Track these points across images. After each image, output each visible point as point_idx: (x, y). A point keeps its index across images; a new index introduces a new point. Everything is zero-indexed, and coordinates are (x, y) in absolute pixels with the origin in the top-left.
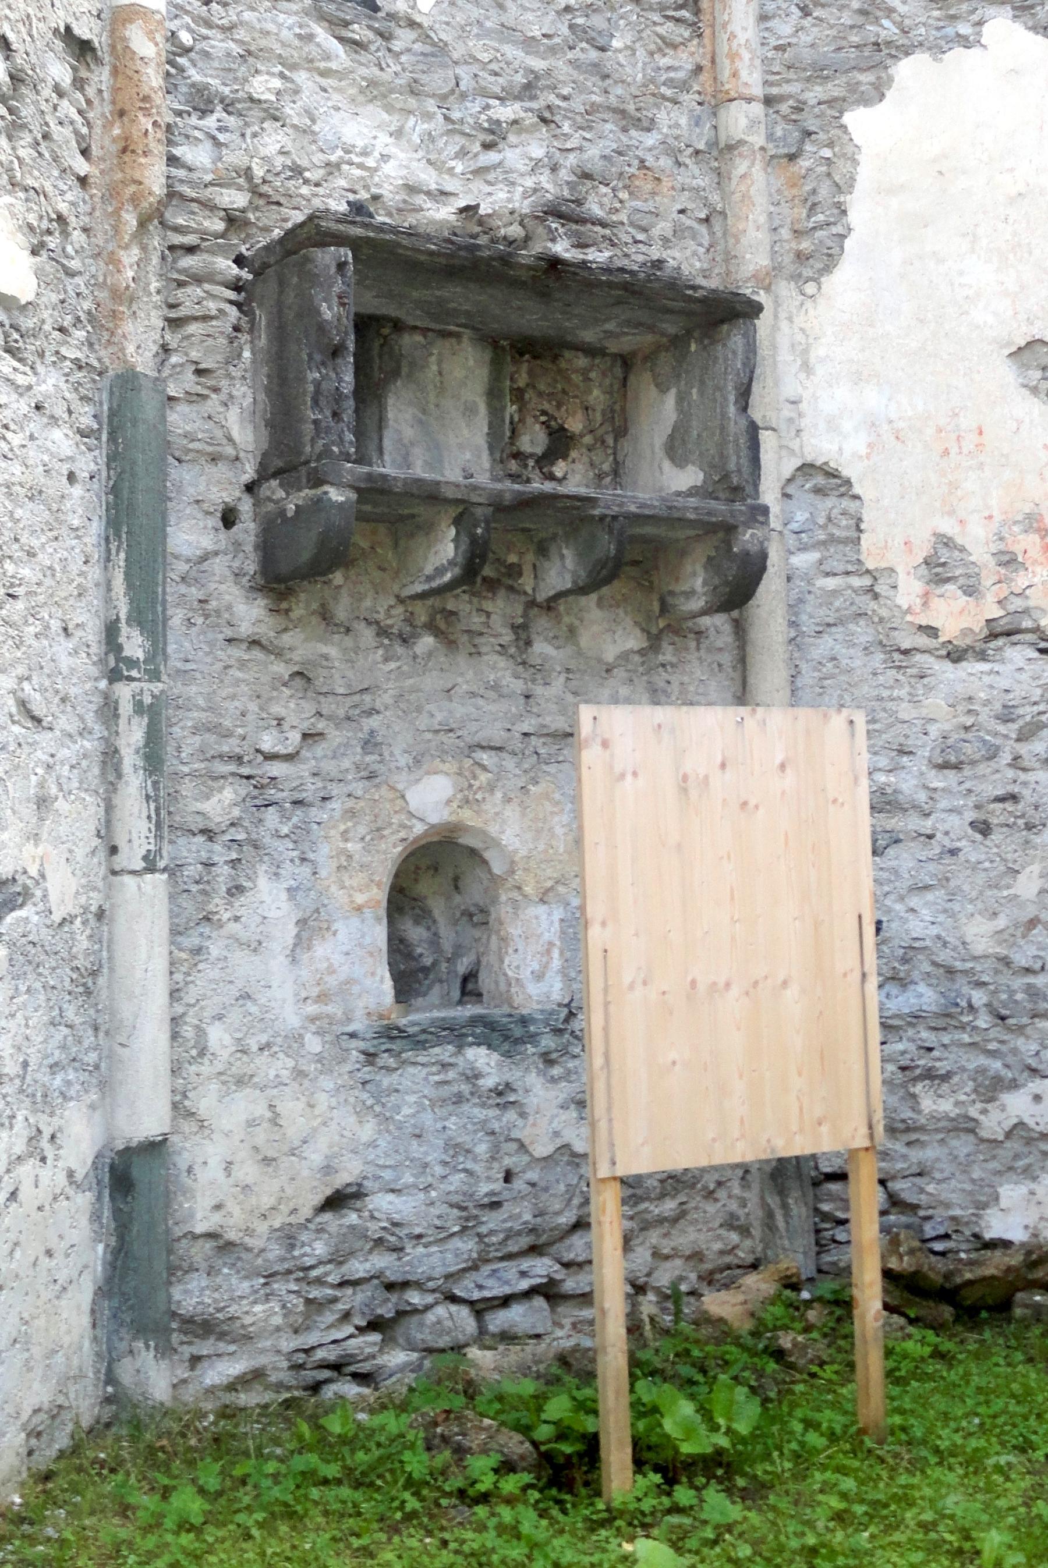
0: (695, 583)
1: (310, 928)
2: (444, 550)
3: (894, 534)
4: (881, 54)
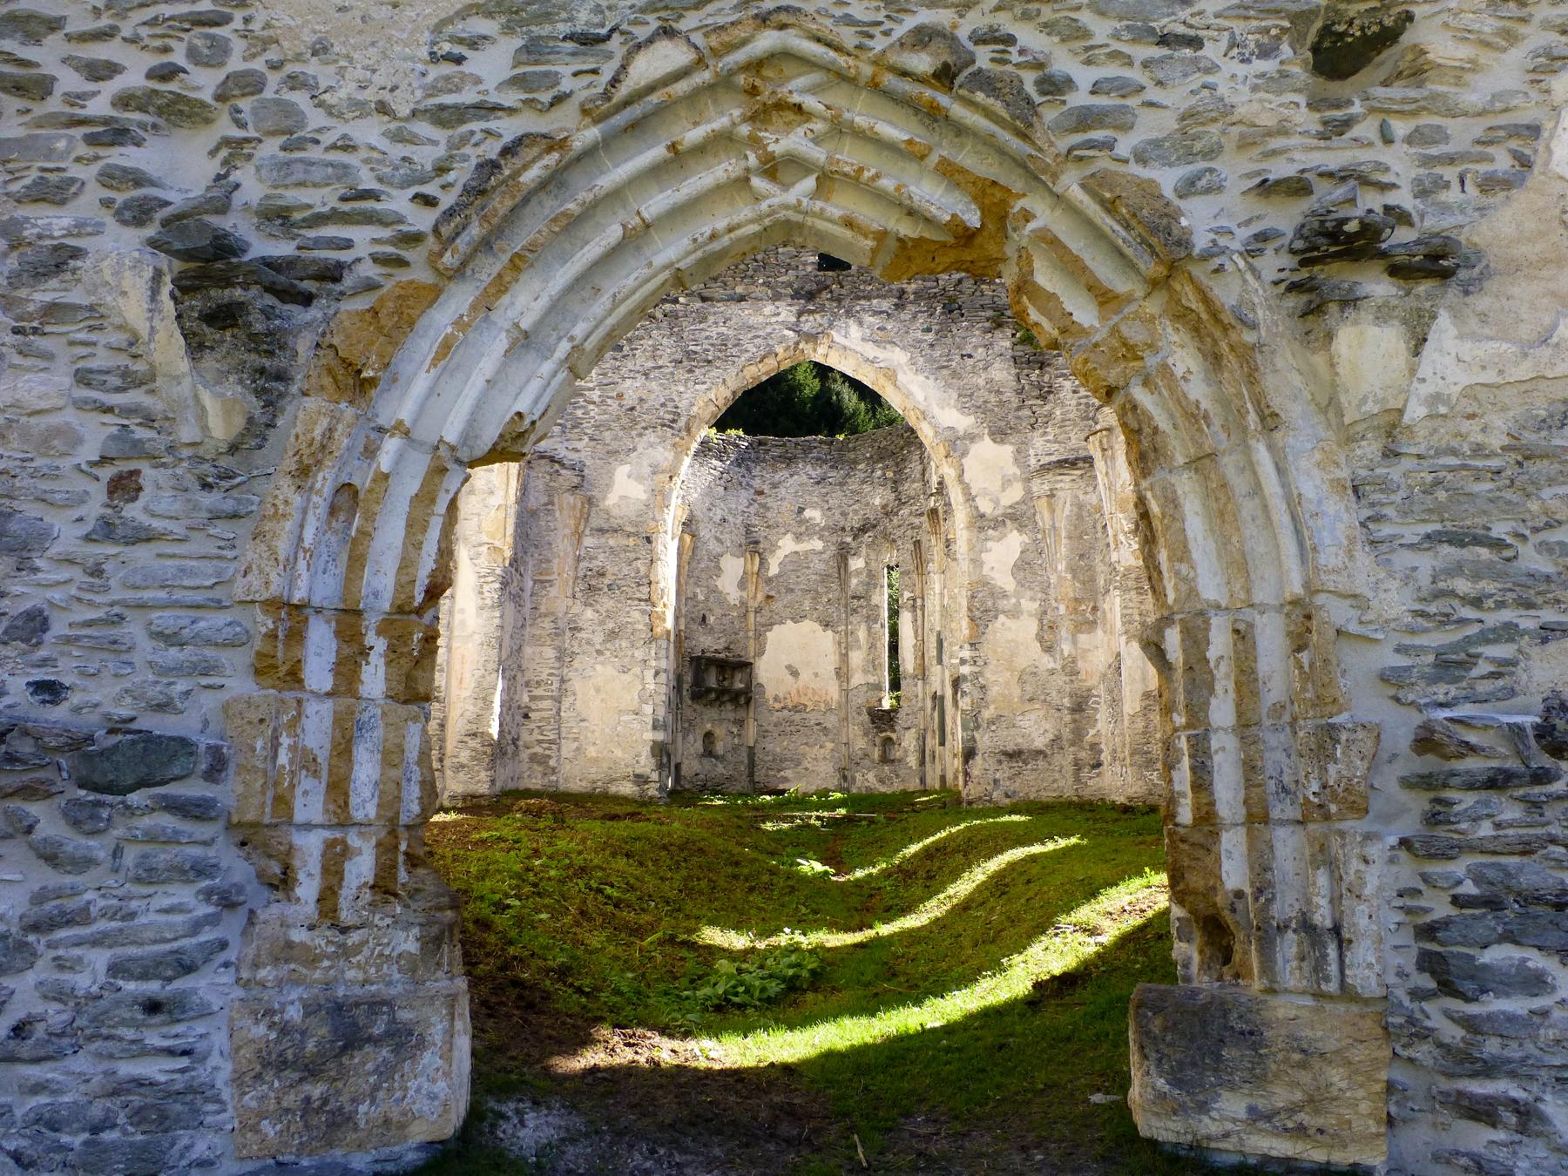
0: (742, 700)
2: (713, 696)
3: (770, 693)
4: (772, 624)
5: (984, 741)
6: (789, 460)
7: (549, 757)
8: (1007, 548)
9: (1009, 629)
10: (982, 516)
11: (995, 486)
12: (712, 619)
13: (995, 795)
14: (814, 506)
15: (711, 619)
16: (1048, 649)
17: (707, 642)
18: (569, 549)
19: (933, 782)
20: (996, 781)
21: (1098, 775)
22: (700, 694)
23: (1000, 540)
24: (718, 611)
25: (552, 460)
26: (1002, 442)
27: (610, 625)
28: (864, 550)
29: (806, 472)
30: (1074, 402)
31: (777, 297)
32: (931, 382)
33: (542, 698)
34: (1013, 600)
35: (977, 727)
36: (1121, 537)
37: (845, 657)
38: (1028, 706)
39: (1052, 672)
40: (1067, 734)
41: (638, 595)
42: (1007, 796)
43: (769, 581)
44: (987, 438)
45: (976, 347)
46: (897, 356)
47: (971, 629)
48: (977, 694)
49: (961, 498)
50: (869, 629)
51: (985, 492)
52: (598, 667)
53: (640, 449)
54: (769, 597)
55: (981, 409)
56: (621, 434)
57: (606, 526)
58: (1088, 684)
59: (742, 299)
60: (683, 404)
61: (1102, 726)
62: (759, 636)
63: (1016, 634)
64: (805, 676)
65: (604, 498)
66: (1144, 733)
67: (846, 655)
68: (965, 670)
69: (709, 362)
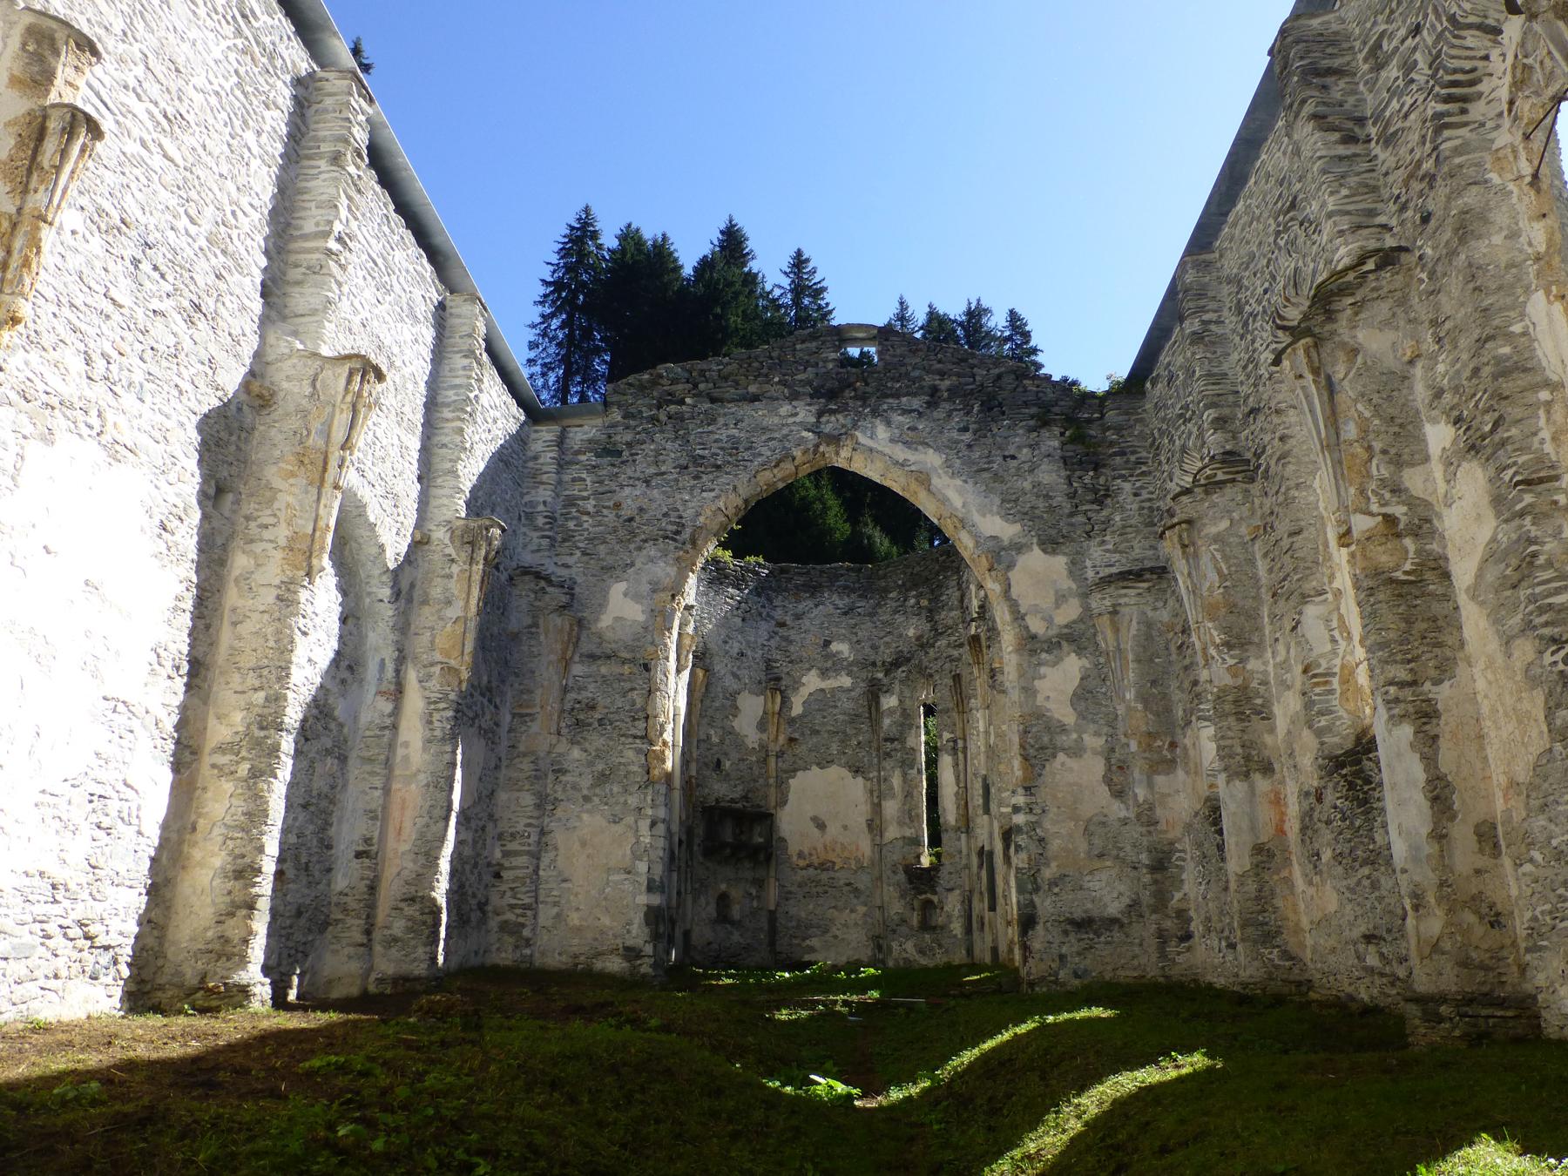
0: (762, 857)
1: (708, 903)
2: (728, 851)
3: (793, 849)
4: (795, 771)
5: (1045, 905)
6: (813, 589)
7: (523, 925)
8: (1061, 678)
9: (1071, 770)
10: (1034, 637)
11: (1047, 602)
12: (728, 764)
13: (1062, 974)
14: (842, 638)
15: (727, 764)
16: (1119, 794)
17: (720, 790)
18: (555, 678)
19: (983, 954)
20: (1062, 957)
21: (1189, 949)
22: (713, 849)
23: (1055, 664)
24: (735, 755)
25: (538, 576)
26: (1054, 552)
27: (600, 767)
28: (897, 687)
29: (834, 601)
30: (1135, 506)
31: (794, 397)
32: (970, 487)
33: (516, 853)
34: (1074, 736)
35: (1037, 890)
36: (1212, 651)
37: (877, 808)
38: (1097, 864)
39: (1125, 822)
40: (1146, 898)
41: (633, 731)
42: (1076, 976)
43: (792, 721)
44: (1036, 548)
45: (1019, 448)
46: (931, 459)
47: (1025, 770)
48: (1035, 849)
49: (1008, 617)
50: (905, 775)
51: (1036, 609)
52: (585, 816)
53: (638, 565)
54: (792, 740)
55: (1027, 516)
56: (617, 547)
57: (598, 652)
58: (1170, 836)
59: (755, 398)
60: (688, 514)
61: (1191, 886)
62: (782, 785)
63: (1079, 774)
64: (833, 829)
65: (597, 620)
66: (1258, 898)
67: (879, 805)
68: (1020, 819)
69: (718, 467)
